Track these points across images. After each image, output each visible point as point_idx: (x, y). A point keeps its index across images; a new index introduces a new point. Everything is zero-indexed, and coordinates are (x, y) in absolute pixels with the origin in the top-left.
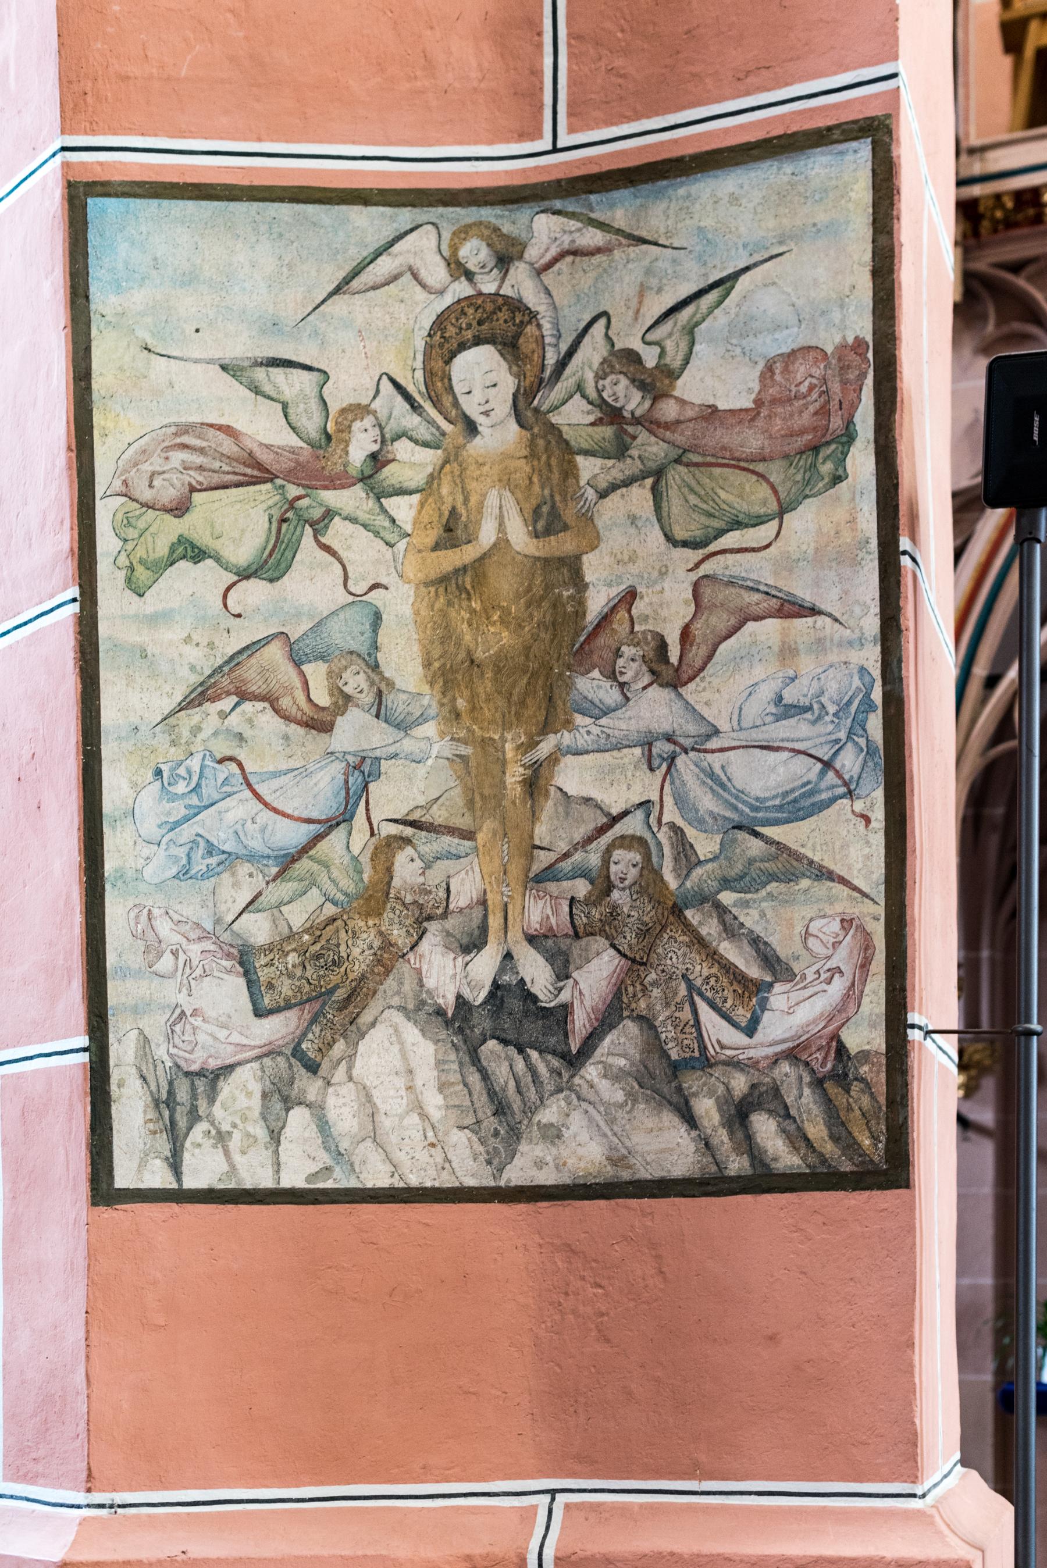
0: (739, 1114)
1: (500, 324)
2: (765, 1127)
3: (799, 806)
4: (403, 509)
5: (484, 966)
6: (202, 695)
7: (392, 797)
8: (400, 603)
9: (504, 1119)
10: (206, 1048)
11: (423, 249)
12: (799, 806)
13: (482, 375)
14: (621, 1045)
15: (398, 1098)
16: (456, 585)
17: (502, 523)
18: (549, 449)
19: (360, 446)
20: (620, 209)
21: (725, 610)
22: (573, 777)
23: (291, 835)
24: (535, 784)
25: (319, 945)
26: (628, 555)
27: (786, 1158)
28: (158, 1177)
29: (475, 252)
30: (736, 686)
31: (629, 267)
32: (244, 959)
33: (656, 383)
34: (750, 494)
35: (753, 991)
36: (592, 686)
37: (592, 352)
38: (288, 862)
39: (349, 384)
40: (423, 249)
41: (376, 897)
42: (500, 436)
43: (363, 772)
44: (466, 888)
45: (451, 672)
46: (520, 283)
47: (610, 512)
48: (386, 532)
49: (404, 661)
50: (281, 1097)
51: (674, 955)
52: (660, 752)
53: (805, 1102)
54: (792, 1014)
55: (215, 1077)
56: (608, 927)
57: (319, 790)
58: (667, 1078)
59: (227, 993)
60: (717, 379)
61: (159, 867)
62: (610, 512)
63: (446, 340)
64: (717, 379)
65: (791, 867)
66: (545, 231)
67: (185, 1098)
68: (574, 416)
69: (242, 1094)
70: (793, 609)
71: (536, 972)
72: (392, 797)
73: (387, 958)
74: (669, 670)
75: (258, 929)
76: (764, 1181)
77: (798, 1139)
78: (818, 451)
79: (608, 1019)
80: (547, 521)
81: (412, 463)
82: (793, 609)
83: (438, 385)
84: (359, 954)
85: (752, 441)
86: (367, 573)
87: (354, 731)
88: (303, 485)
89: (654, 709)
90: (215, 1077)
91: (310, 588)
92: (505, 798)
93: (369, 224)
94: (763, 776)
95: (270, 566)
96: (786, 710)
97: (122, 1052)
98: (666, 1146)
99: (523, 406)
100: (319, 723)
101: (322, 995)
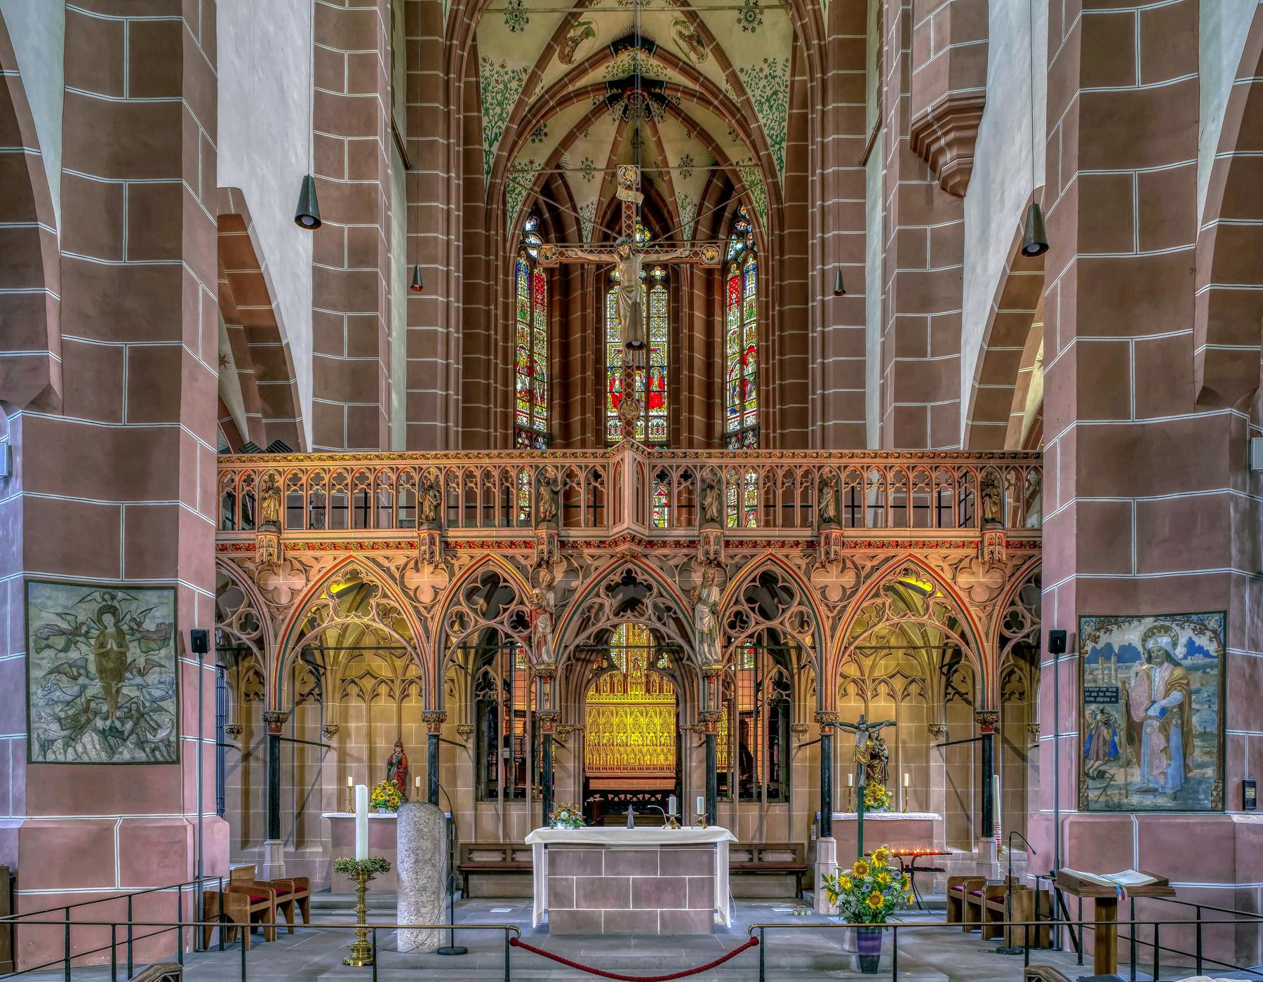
0: (153, 751)
1: (113, 611)
2: (157, 753)
3: (163, 699)
4: (93, 642)
5: (108, 723)
6: (51, 672)
7: (90, 692)
8: (92, 657)
9: (112, 750)
10: (52, 735)
11: (97, 595)
12: (163, 699)
13: (108, 619)
14: (133, 738)
15: (90, 746)
16: (103, 655)
17: (112, 645)
18: (120, 633)
19: (84, 629)
20: (133, 593)
21: (150, 664)
22: (125, 691)
23: (69, 698)
24: (118, 691)
25: (75, 718)
26: (134, 653)
27: (161, 759)
28: (41, 759)
29: (107, 597)
30: (153, 678)
31: (134, 606)
32: (59, 720)
33: (139, 624)
34: (154, 646)
35: (155, 730)
36: (128, 675)
37: (128, 617)
38: (68, 703)
39: (81, 618)
40: (97, 595)
41: (86, 710)
42: (111, 630)
43: (84, 687)
44: (105, 708)
45: (102, 671)
46: (115, 603)
47: (131, 645)
48: (89, 645)
49: (92, 668)
50: (66, 745)
51: (142, 723)
52: (140, 687)
53: (164, 749)
54: (162, 734)
55: (53, 741)
56: (131, 717)
57: (76, 689)
58: (141, 744)
59: (55, 726)
60: (149, 625)
61: (42, 703)
62: (131, 645)
63: (102, 612)
64: (149, 625)
65: (161, 709)
66: (120, 595)
67: (46, 745)
68: (125, 628)
69: (59, 744)
70: (161, 666)
71: (118, 724)
72: (90, 692)
73: (89, 721)
74: (142, 674)
75: (62, 715)
76: (157, 763)
77: (162, 756)
78: (165, 639)
79: (131, 734)
80: (120, 645)
81: (94, 633)
82: (161, 666)
83: (100, 620)
84: (83, 719)
85: (155, 637)
86: (84, 652)
87: (82, 680)
88: (73, 635)
89: (139, 680)
90: (53, 741)
91: (73, 655)
92: (111, 694)
93: (86, 591)
94: (157, 693)
95: (66, 649)
96: (161, 683)
97: (34, 736)
98: (141, 756)
99: (116, 624)
100: (75, 678)
101: (75, 727)
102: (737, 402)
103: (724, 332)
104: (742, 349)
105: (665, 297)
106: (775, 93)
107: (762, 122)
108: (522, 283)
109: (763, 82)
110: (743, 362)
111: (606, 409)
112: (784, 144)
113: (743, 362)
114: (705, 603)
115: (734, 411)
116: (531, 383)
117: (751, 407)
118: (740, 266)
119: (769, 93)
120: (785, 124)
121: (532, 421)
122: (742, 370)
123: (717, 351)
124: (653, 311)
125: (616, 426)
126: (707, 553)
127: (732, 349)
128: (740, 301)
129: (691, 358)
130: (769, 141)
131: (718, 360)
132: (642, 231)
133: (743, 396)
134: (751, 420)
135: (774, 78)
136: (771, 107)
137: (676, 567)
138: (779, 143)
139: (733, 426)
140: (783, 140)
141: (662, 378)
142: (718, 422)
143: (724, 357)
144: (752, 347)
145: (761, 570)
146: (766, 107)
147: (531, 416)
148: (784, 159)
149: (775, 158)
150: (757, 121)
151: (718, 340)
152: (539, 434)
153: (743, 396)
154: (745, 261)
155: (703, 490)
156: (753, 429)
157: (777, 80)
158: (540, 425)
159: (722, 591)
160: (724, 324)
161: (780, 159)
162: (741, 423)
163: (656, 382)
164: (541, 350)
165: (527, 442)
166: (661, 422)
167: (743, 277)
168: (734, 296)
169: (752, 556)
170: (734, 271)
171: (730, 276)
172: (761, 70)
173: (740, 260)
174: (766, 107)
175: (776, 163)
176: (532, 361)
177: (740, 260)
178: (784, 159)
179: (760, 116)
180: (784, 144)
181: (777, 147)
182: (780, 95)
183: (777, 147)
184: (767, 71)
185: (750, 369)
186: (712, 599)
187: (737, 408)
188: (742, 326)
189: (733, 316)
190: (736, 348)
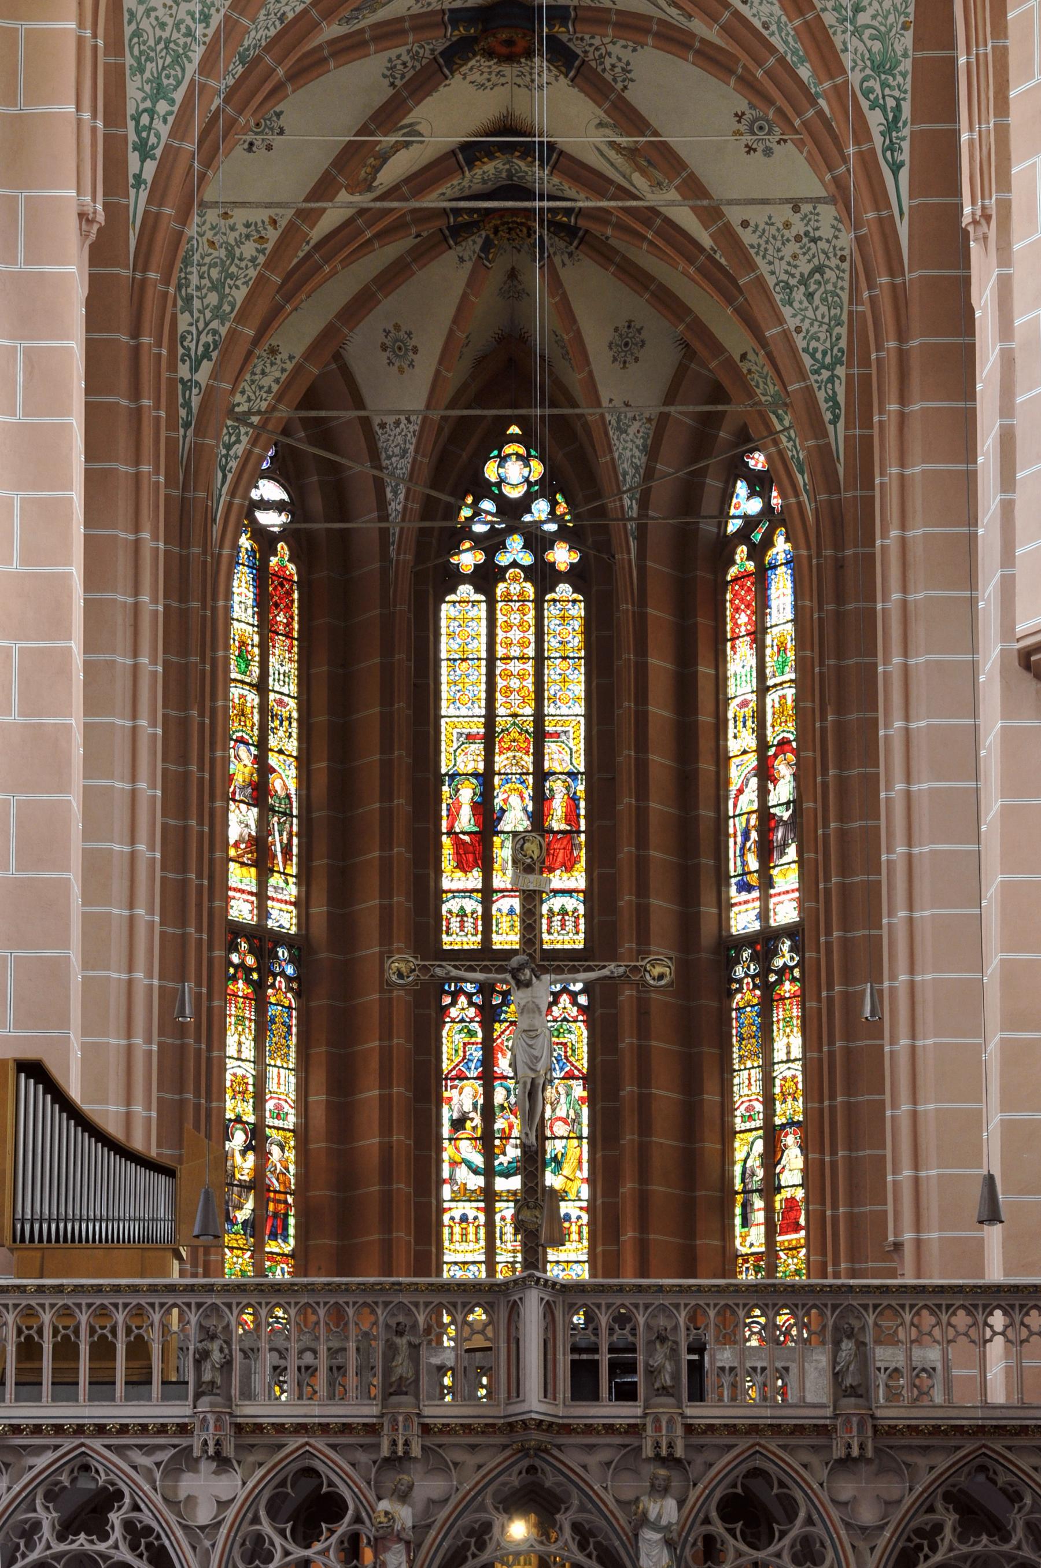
102: (753, 864)
103: (721, 701)
104: (763, 745)
105: (578, 610)
106: (819, 269)
107: (792, 323)
108: (243, 590)
109: (793, 247)
110: (765, 774)
111: (439, 872)
112: (841, 371)
113: (765, 774)
114: (656, 1527)
115: (745, 887)
116: (262, 822)
117: (787, 877)
118: (758, 552)
119: (806, 268)
120: (843, 331)
121: (263, 913)
122: (763, 793)
123: (705, 745)
124: (551, 643)
125: (462, 914)
126: (657, 1446)
127: (740, 741)
128: (758, 635)
129: (642, 767)
130: (807, 361)
131: (706, 766)
132: (525, 460)
133: (767, 852)
134: (786, 912)
135: (814, 240)
136: (810, 296)
137: (608, 1464)
138: (831, 367)
139: (743, 920)
140: (837, 362)
141: (574, 800)
142: (709, 910)
143: (722, 759)
144: (784, 743)
145: (744, 1468)
146: (799, 294)
147: (261, 896)
148: (841, 399)
149: (821, 395)
150: (780, 320)
151: (705, 718)
152: (279, 938)
153: (767, 852)
154: (768, 542)
155: (650, 1343)
156: (791, 931)
157: (823, 245)
158: (283, 918)
159: (681, 1504)
160: (720, 681)
161: (833, 398)
162: (764, 915)
163: (558, 806)
164: (285, 741)
165: (250, 961)
166: (572, 903)
167: (762, 576)
168: (743, 619)
169: (730, 1447)
170: (742, 561)
171: (733, 571)
172: (787, 225)
173: (757, 537)
174: (799, 294)
175: (823, 406)
176: (264, 769)
177: (757, 537)
178: (841, 399)
179: (787, 311)
180: (841, 371)
181: (825, 374)
182: (829, 274)
183: (825, 374)
184: (799, 227)
185: (783, 791)
186: (664, 1522)
187: (753, 879)
188: (763, 690)
189: (740, 662)
190: (749, 740)
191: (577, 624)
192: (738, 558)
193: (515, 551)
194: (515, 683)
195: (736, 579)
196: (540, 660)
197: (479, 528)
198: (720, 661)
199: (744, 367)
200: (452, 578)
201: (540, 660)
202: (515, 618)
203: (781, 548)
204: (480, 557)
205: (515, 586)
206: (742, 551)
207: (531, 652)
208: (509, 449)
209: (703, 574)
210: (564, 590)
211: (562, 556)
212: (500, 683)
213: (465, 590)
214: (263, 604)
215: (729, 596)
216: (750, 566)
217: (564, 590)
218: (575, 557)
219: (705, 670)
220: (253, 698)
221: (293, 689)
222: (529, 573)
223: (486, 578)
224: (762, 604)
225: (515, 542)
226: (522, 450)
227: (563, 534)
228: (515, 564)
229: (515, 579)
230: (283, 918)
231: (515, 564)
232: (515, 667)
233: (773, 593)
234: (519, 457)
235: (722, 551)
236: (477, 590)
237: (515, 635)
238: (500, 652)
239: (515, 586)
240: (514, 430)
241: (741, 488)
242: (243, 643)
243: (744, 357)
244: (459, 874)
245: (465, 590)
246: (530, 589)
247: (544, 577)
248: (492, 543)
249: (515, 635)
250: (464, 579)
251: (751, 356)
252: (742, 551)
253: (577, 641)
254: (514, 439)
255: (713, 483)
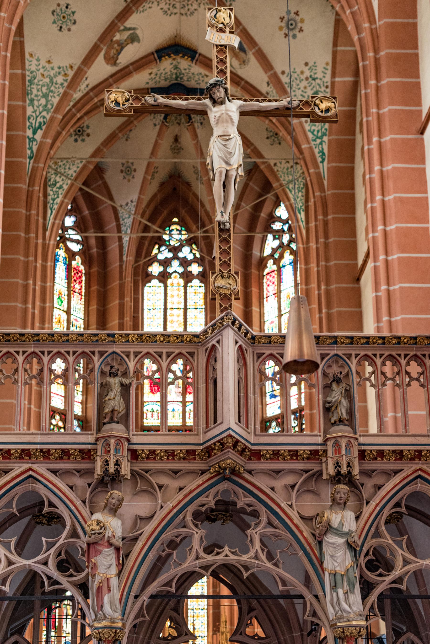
118: (277, 262)
154: (281, 257)
170: (271, 266)
171: (266, 271)
173: (276, 256)
177: (276, 256)
191: (202, 296)
192: (268, 265)
193: (175, 266)
194: (175, 318)
195: (268, 274)
196: (186, 309)
197: (161, 257)
198: (261, 305)
199: (275, 169)
200: (148, 277)
201: (186, 309)
202: (175, 293)
203: (288, 258)
204: (161, 269)
205: (175, 281)
206: (271, 262)
207: (182, 306)
208: (173, 227)
209: (254, 271)
210: (196, 282)
211: (195, 269)
212: (169, 318)
213: (155, 282)
214: (68, 277)
215: (265, 281)
216: (275, 267)
217: (196, 282)
218: (201, 269)
219: (255, 309)
220: (64, 316)
221: (82, 316)
222: (182, 275)
223: (164, 277)
224: (280, 281)
225: (175, 264)
226: (179, 228)
227: (195, 260)
228: (175, 272)
229: (175, 277)
230: (78, 410)
231: (175, 272)
232: (175, 312)
233: (283, 277)
234: (177, 230)
235: (262, 263)
236: (160, 281)
237: (176, 299)
238: (169, 306)
239: (175, 281)
240: (175, 220)
241: (270, 237)
242: (60, 293)
243: (275, 164)
244: (151, 394)
245: (155, 282)
246: (182, 282)
247: (187, 277)
248: (166, 263)
249: (176, 299)
250: (154, 277)
251: (278, 164)
252: (271, 262)
253: (201, 303)
254: (175, 223)
255: (258, 236)
